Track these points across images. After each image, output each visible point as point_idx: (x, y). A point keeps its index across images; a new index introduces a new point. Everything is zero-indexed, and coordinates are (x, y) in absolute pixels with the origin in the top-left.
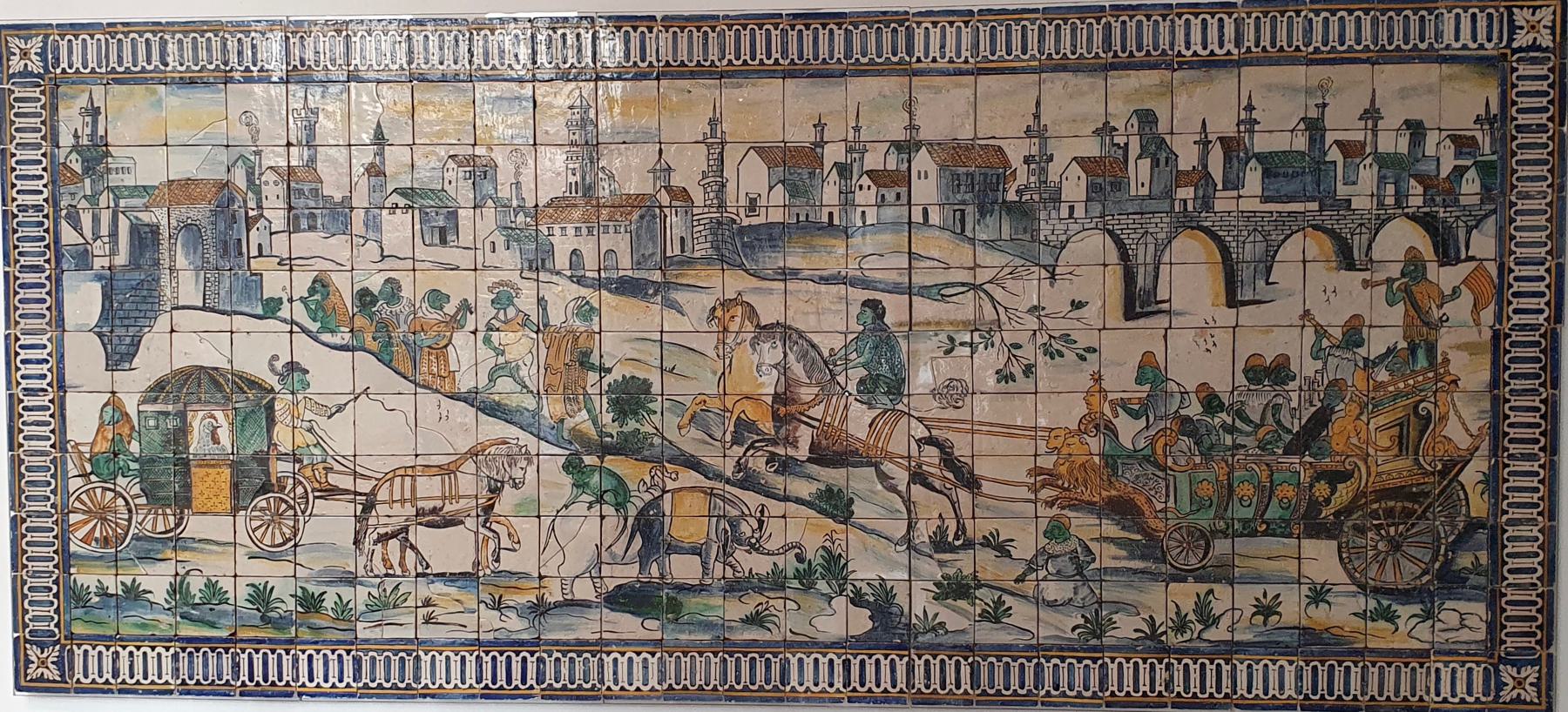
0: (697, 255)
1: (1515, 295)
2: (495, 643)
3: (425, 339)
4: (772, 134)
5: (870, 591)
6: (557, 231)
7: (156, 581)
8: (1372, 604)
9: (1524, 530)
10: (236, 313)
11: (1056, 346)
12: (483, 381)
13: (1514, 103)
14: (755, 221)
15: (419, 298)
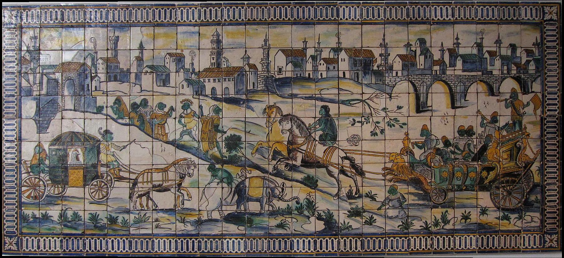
0: (259, 89)
1: (548, 105)
2: (183, 235)
4: (287, 45)
5: (324, 214)
6: (207, 80)
7: (54, 212)
8: (502, 214)
9: (552, 187)
10: (87, 112)
11: (392, 123)
12: (178, 137)
13: (545, 39)
14: (281, 76)
15: (155, 105)
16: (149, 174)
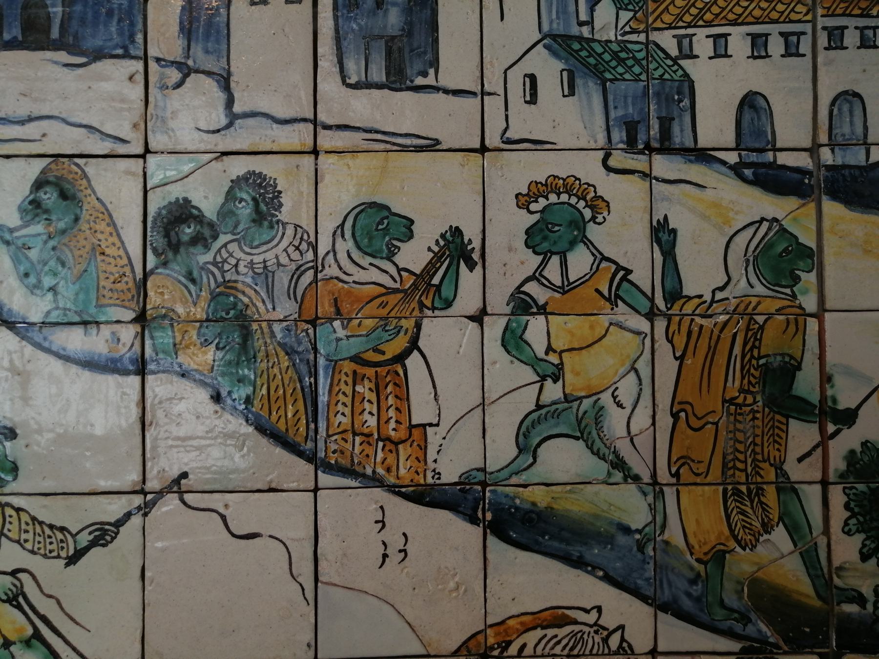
6: (703, 45)
12: (502, 450)
15: (327, 226)
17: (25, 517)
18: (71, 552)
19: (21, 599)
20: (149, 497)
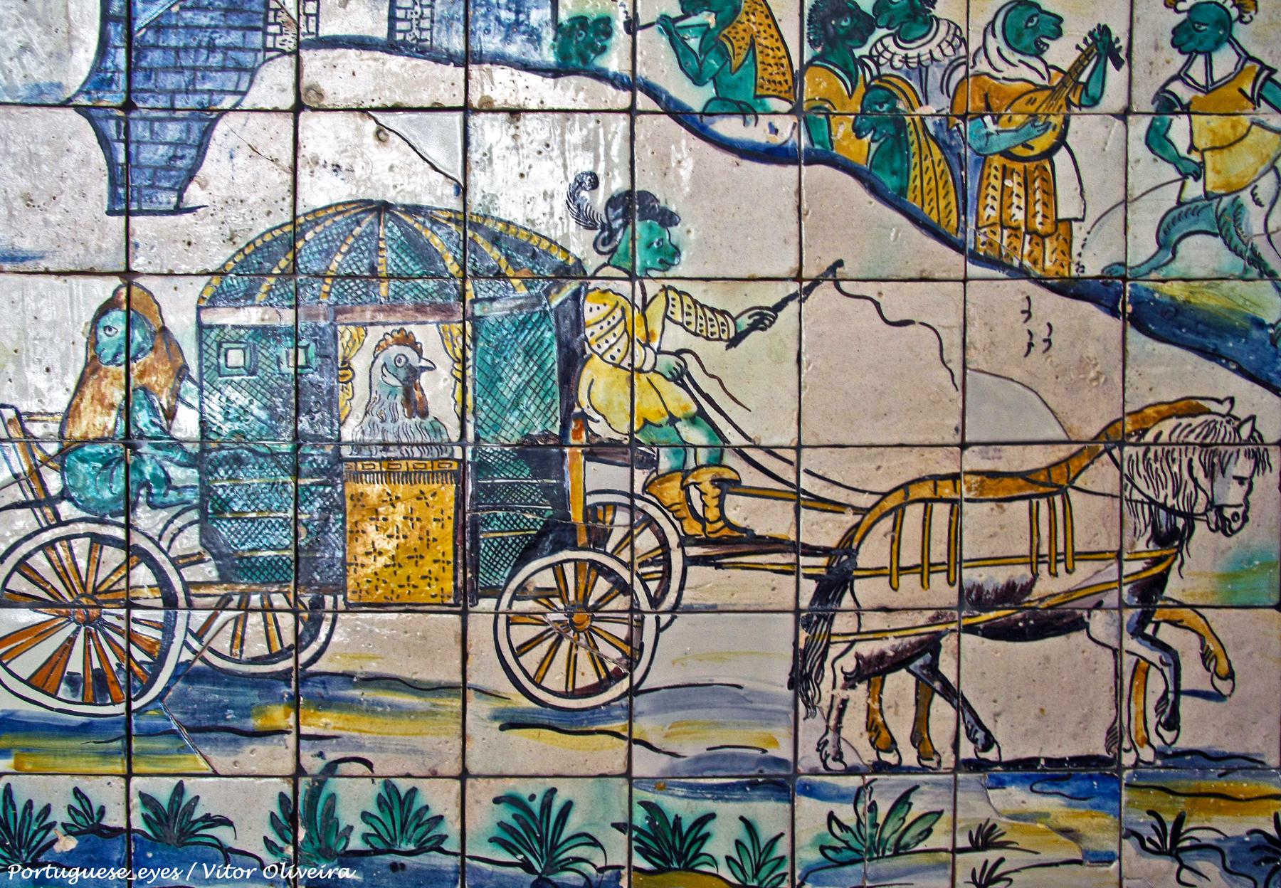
3: (996, 133)
7: (240, 790)
10: (480, 59)
12: (1143, 246)
15: (980, 20)
16: (941, 512)
17: (687, 301)
18: (732, 334)
19: (685, 378)
20: (805, 284)
